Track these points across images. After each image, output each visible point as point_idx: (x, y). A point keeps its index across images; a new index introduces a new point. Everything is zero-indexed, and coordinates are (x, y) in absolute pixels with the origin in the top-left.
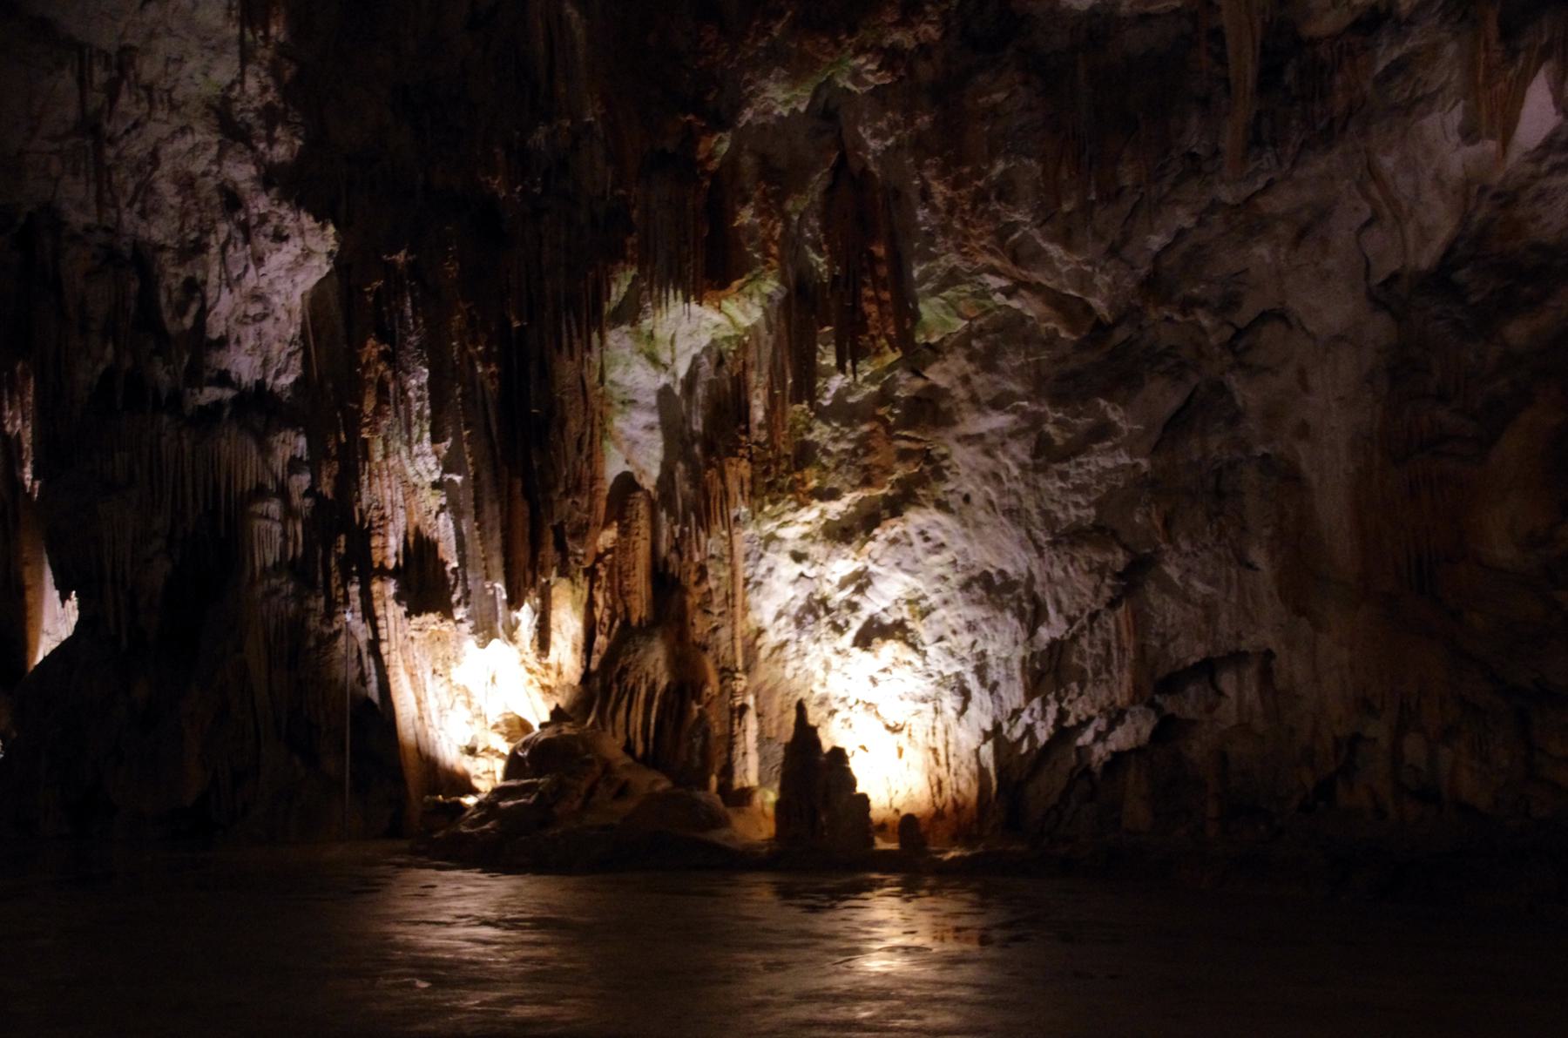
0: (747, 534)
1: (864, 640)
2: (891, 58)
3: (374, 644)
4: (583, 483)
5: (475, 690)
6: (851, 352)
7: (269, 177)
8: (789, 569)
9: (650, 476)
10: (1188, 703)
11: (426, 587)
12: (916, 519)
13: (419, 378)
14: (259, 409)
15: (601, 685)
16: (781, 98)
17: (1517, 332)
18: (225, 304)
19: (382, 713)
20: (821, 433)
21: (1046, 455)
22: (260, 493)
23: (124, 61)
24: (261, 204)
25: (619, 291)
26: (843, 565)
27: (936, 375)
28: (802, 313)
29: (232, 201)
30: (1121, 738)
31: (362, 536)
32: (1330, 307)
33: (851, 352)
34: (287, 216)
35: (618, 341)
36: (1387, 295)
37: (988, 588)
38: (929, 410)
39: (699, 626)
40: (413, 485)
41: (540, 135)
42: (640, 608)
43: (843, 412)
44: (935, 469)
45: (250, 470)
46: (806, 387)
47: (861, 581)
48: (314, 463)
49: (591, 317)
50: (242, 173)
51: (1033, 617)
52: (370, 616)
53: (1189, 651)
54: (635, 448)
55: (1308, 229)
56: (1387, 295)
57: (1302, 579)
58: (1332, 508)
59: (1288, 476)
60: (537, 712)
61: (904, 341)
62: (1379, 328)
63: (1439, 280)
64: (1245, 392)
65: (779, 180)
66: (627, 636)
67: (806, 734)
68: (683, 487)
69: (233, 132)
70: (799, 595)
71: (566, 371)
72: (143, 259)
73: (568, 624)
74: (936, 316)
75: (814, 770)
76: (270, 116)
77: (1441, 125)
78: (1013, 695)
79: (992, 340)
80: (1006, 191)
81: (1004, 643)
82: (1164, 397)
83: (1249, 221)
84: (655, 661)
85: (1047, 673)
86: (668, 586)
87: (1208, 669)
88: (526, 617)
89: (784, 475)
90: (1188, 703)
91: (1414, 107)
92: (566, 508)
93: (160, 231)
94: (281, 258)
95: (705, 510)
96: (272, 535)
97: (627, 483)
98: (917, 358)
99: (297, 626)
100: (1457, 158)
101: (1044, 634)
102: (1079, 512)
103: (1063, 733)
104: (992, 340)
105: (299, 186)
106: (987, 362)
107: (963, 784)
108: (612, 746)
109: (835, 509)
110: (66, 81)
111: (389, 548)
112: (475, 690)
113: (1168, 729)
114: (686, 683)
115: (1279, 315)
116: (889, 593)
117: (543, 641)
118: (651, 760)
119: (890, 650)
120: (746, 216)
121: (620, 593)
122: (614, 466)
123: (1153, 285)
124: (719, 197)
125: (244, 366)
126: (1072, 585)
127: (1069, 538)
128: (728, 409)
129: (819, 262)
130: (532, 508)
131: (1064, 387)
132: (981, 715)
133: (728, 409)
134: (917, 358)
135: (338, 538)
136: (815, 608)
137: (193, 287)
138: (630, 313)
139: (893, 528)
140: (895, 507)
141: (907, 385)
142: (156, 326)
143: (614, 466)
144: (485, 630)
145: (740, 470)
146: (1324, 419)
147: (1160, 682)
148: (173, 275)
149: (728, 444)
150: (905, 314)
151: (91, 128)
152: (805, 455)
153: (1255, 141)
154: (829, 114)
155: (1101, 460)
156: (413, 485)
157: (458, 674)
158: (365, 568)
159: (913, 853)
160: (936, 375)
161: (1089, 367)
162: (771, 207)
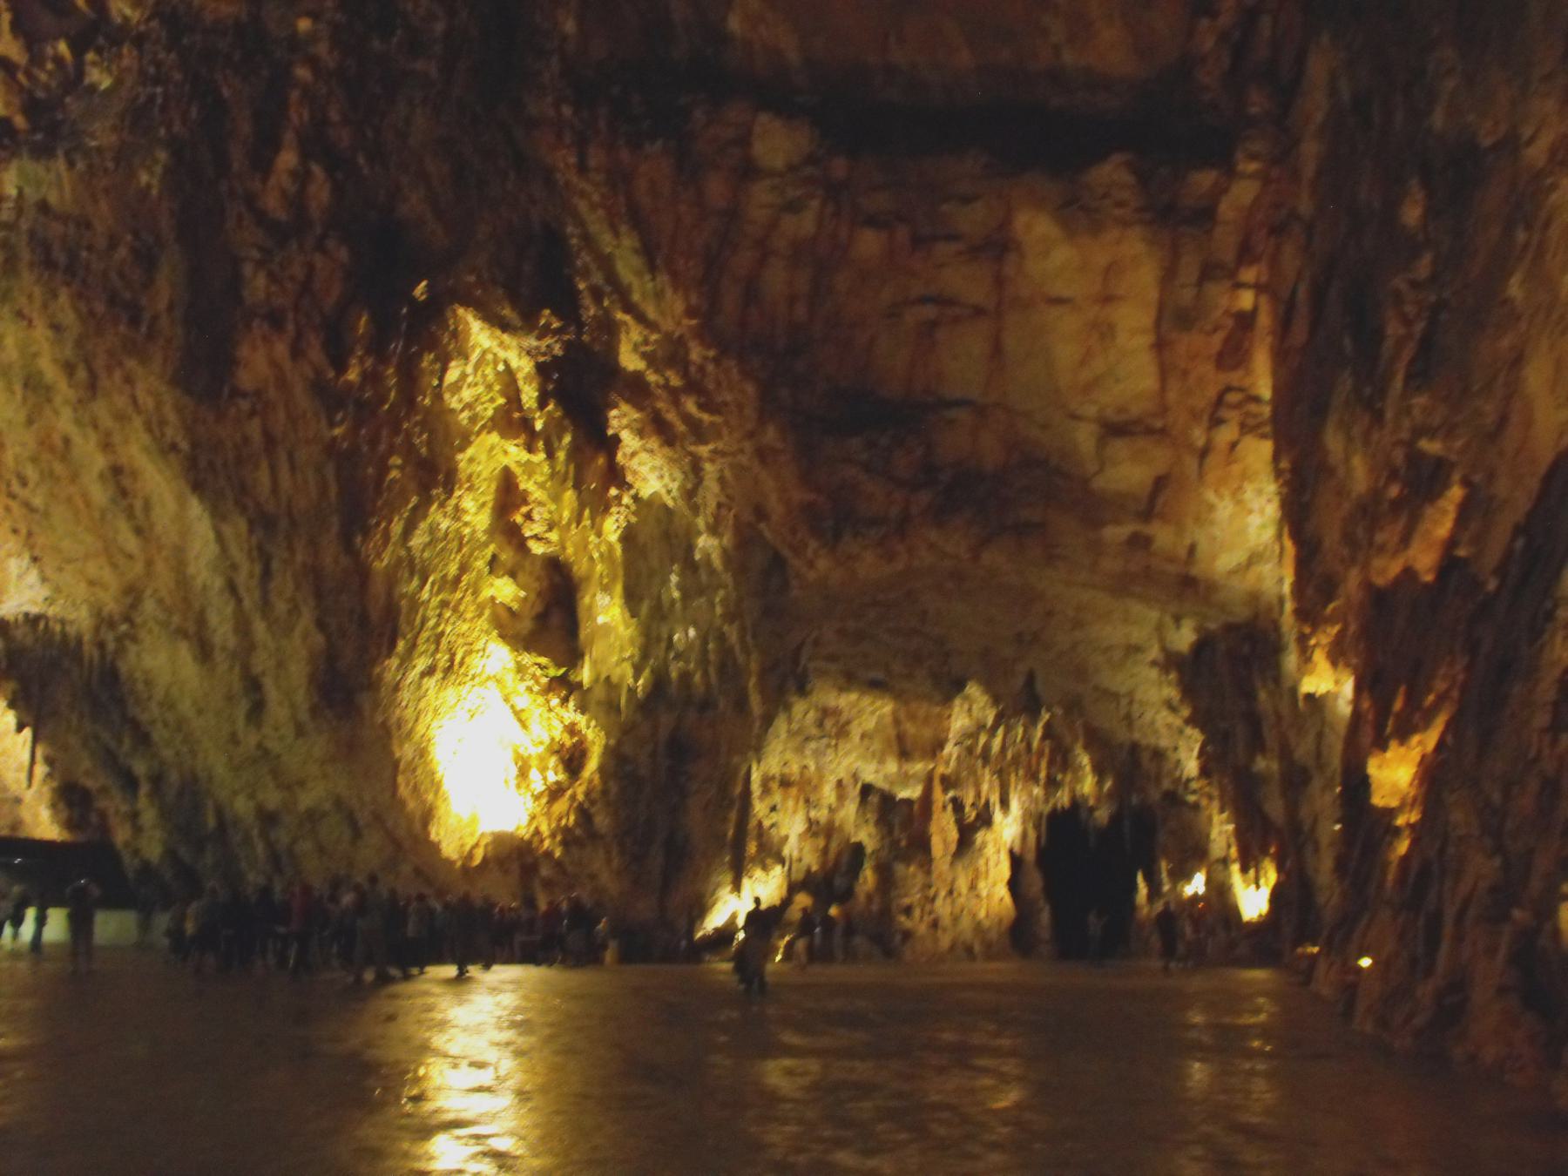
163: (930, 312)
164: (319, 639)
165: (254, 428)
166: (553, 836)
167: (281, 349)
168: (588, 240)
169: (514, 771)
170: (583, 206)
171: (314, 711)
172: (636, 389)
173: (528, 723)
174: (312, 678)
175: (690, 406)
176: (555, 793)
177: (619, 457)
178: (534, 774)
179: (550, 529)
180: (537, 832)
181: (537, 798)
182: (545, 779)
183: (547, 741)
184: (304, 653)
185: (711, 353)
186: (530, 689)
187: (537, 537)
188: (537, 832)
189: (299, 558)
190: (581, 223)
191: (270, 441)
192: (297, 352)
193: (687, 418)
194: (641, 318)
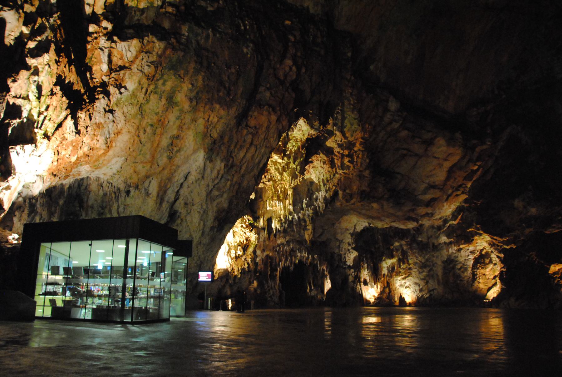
0: (395, 279)
1: (406, 287)
2: (406, 242)
3: (361, 289)
4: (381, 275)
5: (371, 293)
6: (404, 264)
7: (352, 248)
8: (399, 282)
9: (386, 274)
10: (432, 293)
11: (366, 283)
12: (410, 278)
13: (366, 265)
14: (350, 267)
15: (382, 292)
16: (397, 244)
17: (451, 266)
18: (347, 258)
19: (361, 295)
20: (401, 270)
21: (420, 273)
22: (350, 275)
23: (342, 241)
24: (351, 250)
25: (384, 258)
26: (403, 281)
27: (411, 266)
28: (399, 261)
29: (349, 250)
30: (427, 296)
31: (360, 278)
32: (439, 263)
33: (404, 264)
34: (353, 251)
35: (384, 263)
36: (444, 262)
37: (416, 284)
38: (410, 269)
39: (391, 287)
40: (365, 274)
41: (377, 246)
42: (386, 285)
43: (403, 269)
44: (411, 274)
45: (349, 273)
46: (400, 267)
47: (405, 283)
48: (354, 272)
49: (381, 261)
50: (350, 248)
51: (419, 286)
52: (360, 286)
53: (431, 289)
54: (385, 271)
55: (437, 257)
56: (444, 262)
57: (439, 283)
58: (440, 278)
59: (438, 275)
60: (376, 295)
61: (408, 263)
62: (443, 265)
63: (446, 261)
64: (434, 269)
65: (397, 250)
66: (384, 288)
67: (401, 296)
68: (389, 275)
69: (349, 244)
70: (399, 284)
71: (379, 265)
72: (341, 255)
73: (379, 287)
74: (410, 261)
75: (402, 299)
76: (353, 243)
77: (445, 251)
78: (418, 292)
79: (415, 264)
80: (415, 252)
81: (417, 288)
82: (428, 269)
83: (433, 256)
84: (387, 290)
85: (421, 290)
86: (388, 283)
87: (433, 290)
88: (375, 286)
89: (398, 274)
90: (432, 293)
91: (443, 249)
92: (379, 277)
93: (342, 253)
94: (352, 254)
95: (391, 277)
96: (351, 279)
97: (384, 274)
98: (409, 265)
99: (353, 287)
100: (447, 253)
101: (421, 287)
102: (422, 277)
103: (422, 296)
104: (415, 264)
105: (354, 249)
106: (415, 265)
107: (414, 300)
108: (384, 297)
109: (403, 277)
110: (338, 243)
111: (362, 280)
112: (371, 293)
113: (431, 295)
114: (390, 292)
115: (436, 263)
116: (407, 284)
117: (377, 287)
118: (387, 298)
119: (408, 289)
120: (394, 253)
121: (384, 284)
122: (383, 273)
123: (427, 260)
124: (392, 251)
125: (348, 263)
126: (422, 283)
127: (422, 279)
128: (393, 268)
129: (401, 257)
130: (376, 275)
131: (421, 267)
132: (416, 294)
133: (393, 268)
134: (409, 265)
135: (357, 279)
136: (401, 285)
137: (345, 257)
138: (385, 260)
139: (407, 278)
140: (408, 277)
141: (408, 267)
142: (341, 260)
143: (383, 273)
144: (372, 287)
145: (394, 273)
146: (439, 271)
147: (429, 291)
148: (343, 256)
149: (392, 270)
150: (408, 261)
151: (339, 246)
152: (400, 272)
153: (433, 250)
154: (401, 245)
155: (424, 273)
156: (365, 274)
157: (369, 291)
158: (360, 282)
159: (410, 305)
160: (411, 266)
161: (423, 266)
162: (397, 252)
163: (405, 152)
164: (226, 205)
165: (249, 138)
166: (239, 270)
167: (274, 118)
168: (343, 112)
169: (227, 250)
170: (346, 102)
171: (212, 228)
172: (329, 152)
173: (236, 236)
174: (216, 218)
175: (346, 160)
176: (237, 258)
177: (307, 167)
178: (233, 252)
179: (269, 181)
180: (233, 269)
181: (232, 259)
182: (236, 253)
183: (238, 242)
184: (215, 209)
185: (362, 149)
186: (242, 226)
187: (263, 183)
188: (233, 269)
189: (235, 180)
190: (343, 105)
191: (251, 144)
192: (278, 120)
193: (342, 163)
194: (344, 134)
